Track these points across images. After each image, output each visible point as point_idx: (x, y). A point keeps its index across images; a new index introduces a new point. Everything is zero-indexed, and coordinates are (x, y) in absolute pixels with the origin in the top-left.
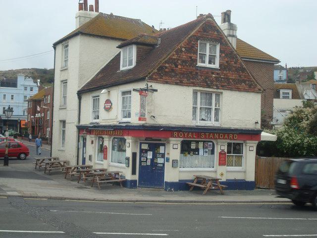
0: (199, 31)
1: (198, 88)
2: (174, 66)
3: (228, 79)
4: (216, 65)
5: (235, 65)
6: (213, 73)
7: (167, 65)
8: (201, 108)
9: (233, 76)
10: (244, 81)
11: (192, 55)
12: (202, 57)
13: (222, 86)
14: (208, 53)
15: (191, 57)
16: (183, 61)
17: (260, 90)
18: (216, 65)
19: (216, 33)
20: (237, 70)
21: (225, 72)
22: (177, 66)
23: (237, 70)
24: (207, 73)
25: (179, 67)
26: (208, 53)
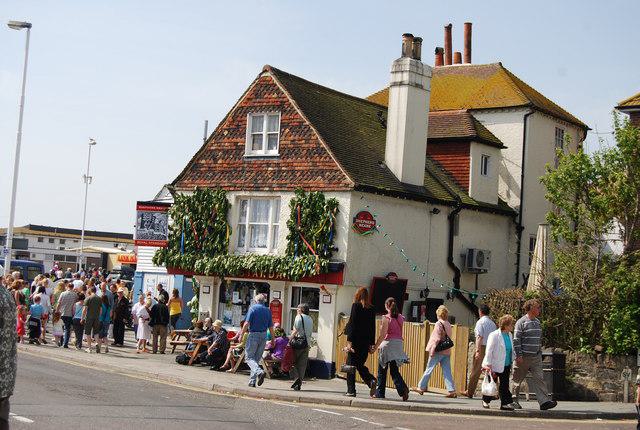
0: (248, 99)
1: (242, 193)
2: (212, 161)
3: (293, 172)
4: (275, 152)
5: (307, 145)
6: (268, 165)
7: (203, 162)
8: (252, 227)
9: (301, 165)
10: (322, 172)
11: (239, 140)
12: (257, 139)
13: (280, 186)
14: (264, 133)
15: (236, 144)
16: (226, 152)
17: (347, 185)
18: (275, 152)
19: (275, 95)
20: (310, 153)
21: (289, 160)
22: (215, 160)
23: (310, 153)
24: (260, 166)
25: (220, 161)
26: (264, 133)
